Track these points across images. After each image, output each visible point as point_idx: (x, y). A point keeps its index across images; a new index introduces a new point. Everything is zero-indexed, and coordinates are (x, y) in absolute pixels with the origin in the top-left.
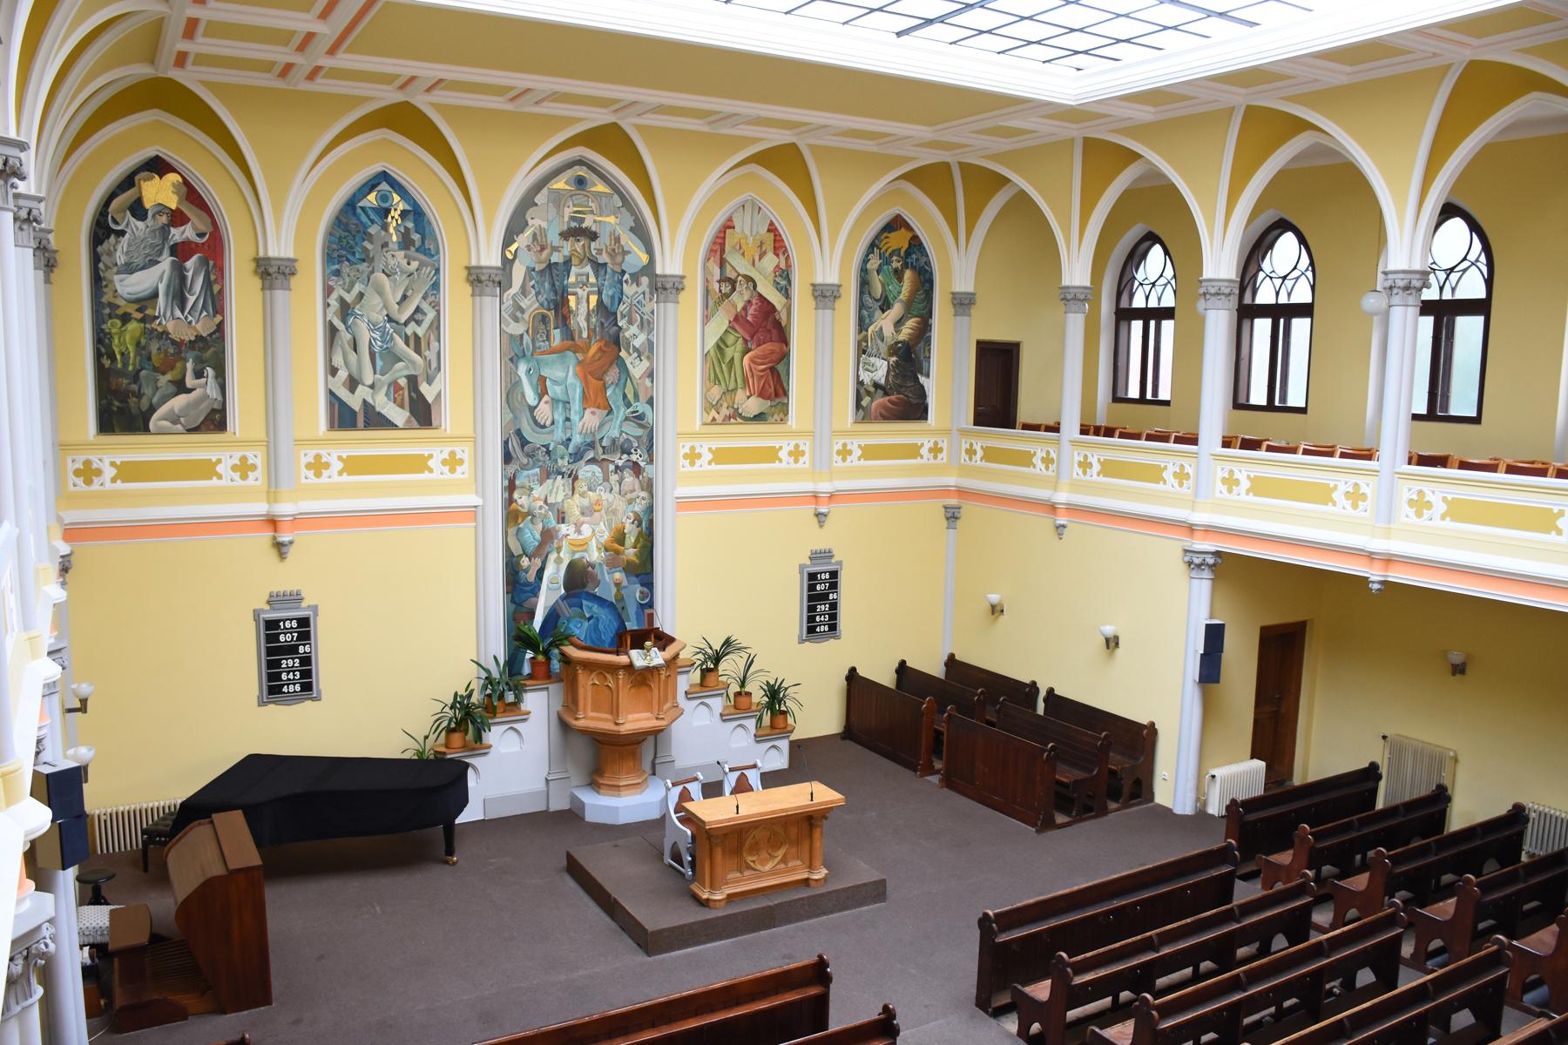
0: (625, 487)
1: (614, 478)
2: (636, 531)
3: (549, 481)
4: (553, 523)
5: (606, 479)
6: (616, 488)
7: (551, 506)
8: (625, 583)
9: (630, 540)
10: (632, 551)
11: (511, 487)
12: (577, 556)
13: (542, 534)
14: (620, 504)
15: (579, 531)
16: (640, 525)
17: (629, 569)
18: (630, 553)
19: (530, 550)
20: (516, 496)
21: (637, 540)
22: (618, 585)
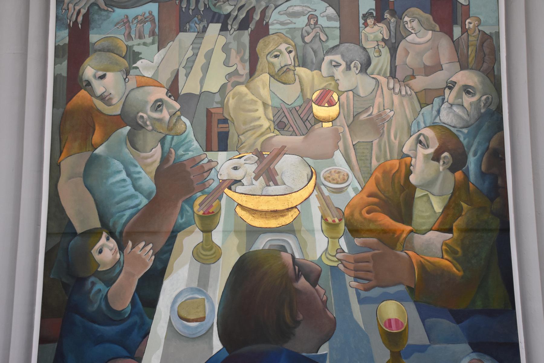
0: (408, 58)
1: (373, 33)
2: (448, 181)
3: (186, 38)
4: (192, 146)
5: (350, 35)
6: (381, 61)
7: (188, 102)
8: (417, 335)
9: (431, 205)
10: (437, 238)
11: (76, 49)
12: (261, 243)
13: (160, 175)
14: (394, 103)
15: (268, 174)
16: (458, 164)
17: (428, 291)
18: (430, 244)
19: (123, 218)
20: (89, 72)
21: (452, 208)
22: (394, 338)
